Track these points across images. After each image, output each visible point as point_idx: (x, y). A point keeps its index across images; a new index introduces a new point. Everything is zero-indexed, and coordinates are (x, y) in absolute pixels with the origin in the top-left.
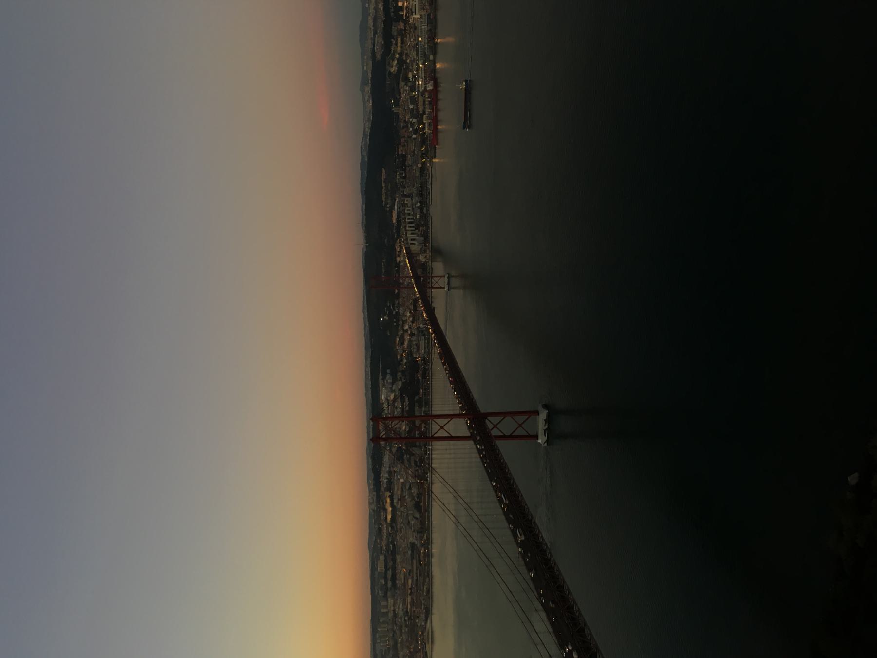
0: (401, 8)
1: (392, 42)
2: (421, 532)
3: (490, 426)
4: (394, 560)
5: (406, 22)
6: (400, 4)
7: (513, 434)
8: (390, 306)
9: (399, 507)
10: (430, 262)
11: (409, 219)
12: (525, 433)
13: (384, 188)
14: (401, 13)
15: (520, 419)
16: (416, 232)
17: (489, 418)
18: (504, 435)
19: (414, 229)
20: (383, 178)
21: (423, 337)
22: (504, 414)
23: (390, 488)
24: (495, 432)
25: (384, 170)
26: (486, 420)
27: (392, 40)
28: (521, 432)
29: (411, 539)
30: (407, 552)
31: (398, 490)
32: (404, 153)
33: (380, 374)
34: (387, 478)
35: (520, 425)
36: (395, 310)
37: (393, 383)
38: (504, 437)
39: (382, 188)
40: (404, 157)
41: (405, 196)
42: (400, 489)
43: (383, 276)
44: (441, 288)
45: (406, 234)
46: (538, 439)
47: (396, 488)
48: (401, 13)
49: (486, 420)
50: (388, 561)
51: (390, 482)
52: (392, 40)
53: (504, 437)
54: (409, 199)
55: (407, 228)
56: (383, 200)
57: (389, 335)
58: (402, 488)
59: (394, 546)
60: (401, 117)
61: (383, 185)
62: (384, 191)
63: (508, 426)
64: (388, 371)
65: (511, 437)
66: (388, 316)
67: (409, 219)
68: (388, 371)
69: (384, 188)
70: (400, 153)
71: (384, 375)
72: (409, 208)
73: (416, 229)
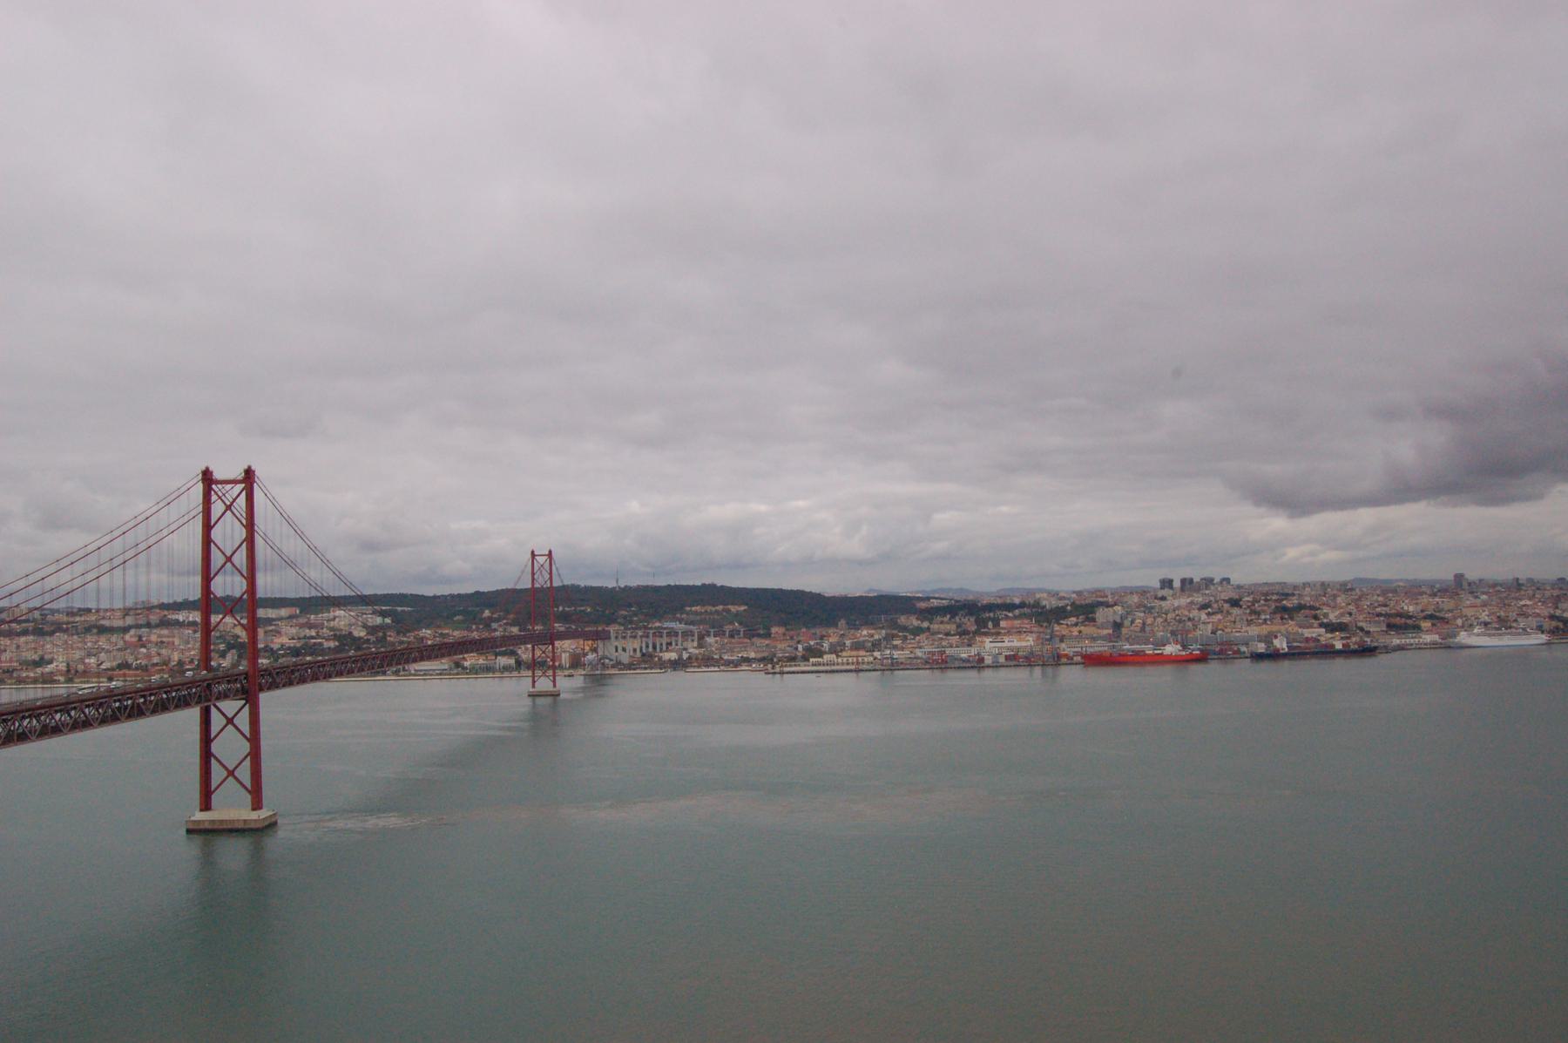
0: (996, 623)
1: (945, 615)
2: (68, 671)
3: (230, 706)
4: (25, 633)
5: (977, 633)
6: (1003, 624)
7: (213, 761)
8: (507, 619)
9: (127, 637)
10: (583, 673)
11: (661, 644)
12: (214, 784)
13: (713, 609)
14: (990, 624)
15: (244, 773)
16: (638, 654)
17: (247, 709)
18: (212, 741)
19: (644, 651)
20: (729, 607)
21: (446, 667)
22: (254, 738)
23: (164, 623)
24: (217, 721)
25: (743, 608)
26: (243, 702)
27: (948, 616)
28: (217, 774)
29: (61, 660)
30: (36, 653)
31: (159, 636)
32: (773, 636)
33: (388, 608)
34: (184, 621)
35: (231, 773)
36: (500, 626)
37: (365, 626)
38: (206, 739)
39: (714, 606)
40: (768, 635)
41: (701, 637)
42: (159, 640)
43: (561, 609)
44: (534, 682)
45: (635, 637)
46: (201, 810)
47: (165, 632)
48: (990, 624)
49: (243, 702)
50: (24, 625)
51: (178, 623)
52: (948, 616)
53: (206, 739)
54: (695, 644)
55: (644, 639)
56: (693, 609)
57: (455, 619)
58: (162, 642)
59: (52, 633)
60: (831, 631)
61: (720, 608)
62: (710, 608)
63: (230, 747)
64: (388, 621)
65: (207, 755)
66: (489, 617)
67: (661, 644)
68: (388, 621)
69: (713, 609)
70: (774, 630)
71: (383, 614)
72: (679, 644)
73: (643, 655)
